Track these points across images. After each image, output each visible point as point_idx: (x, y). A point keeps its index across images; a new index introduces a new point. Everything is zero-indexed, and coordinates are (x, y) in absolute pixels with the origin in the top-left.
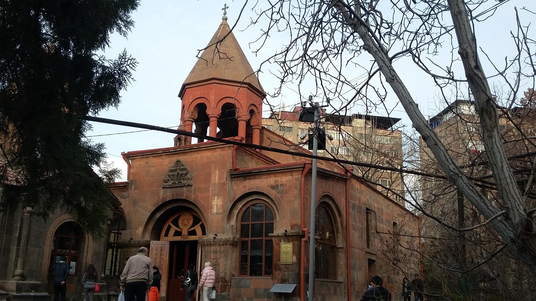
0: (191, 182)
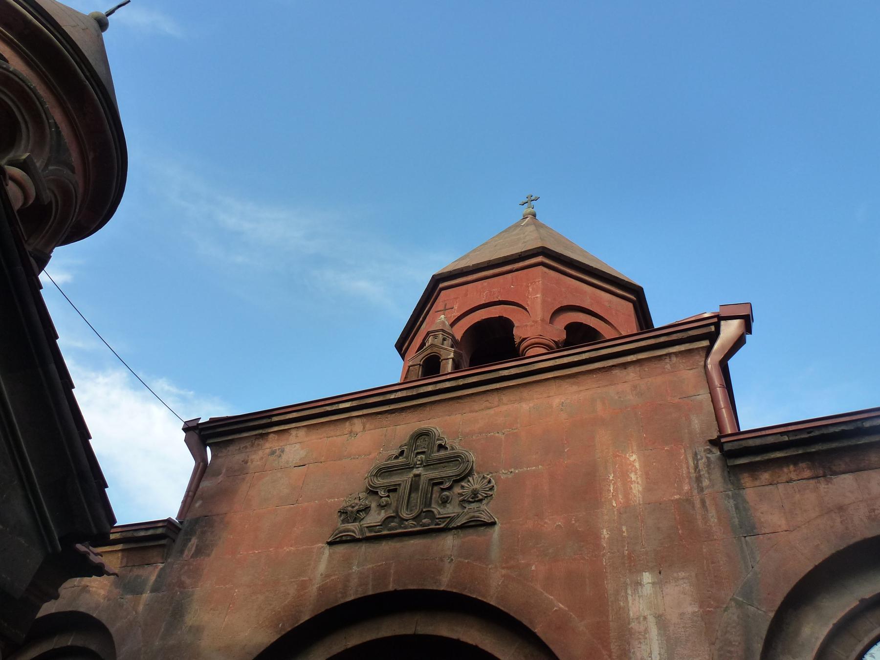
0: (485, 511)
